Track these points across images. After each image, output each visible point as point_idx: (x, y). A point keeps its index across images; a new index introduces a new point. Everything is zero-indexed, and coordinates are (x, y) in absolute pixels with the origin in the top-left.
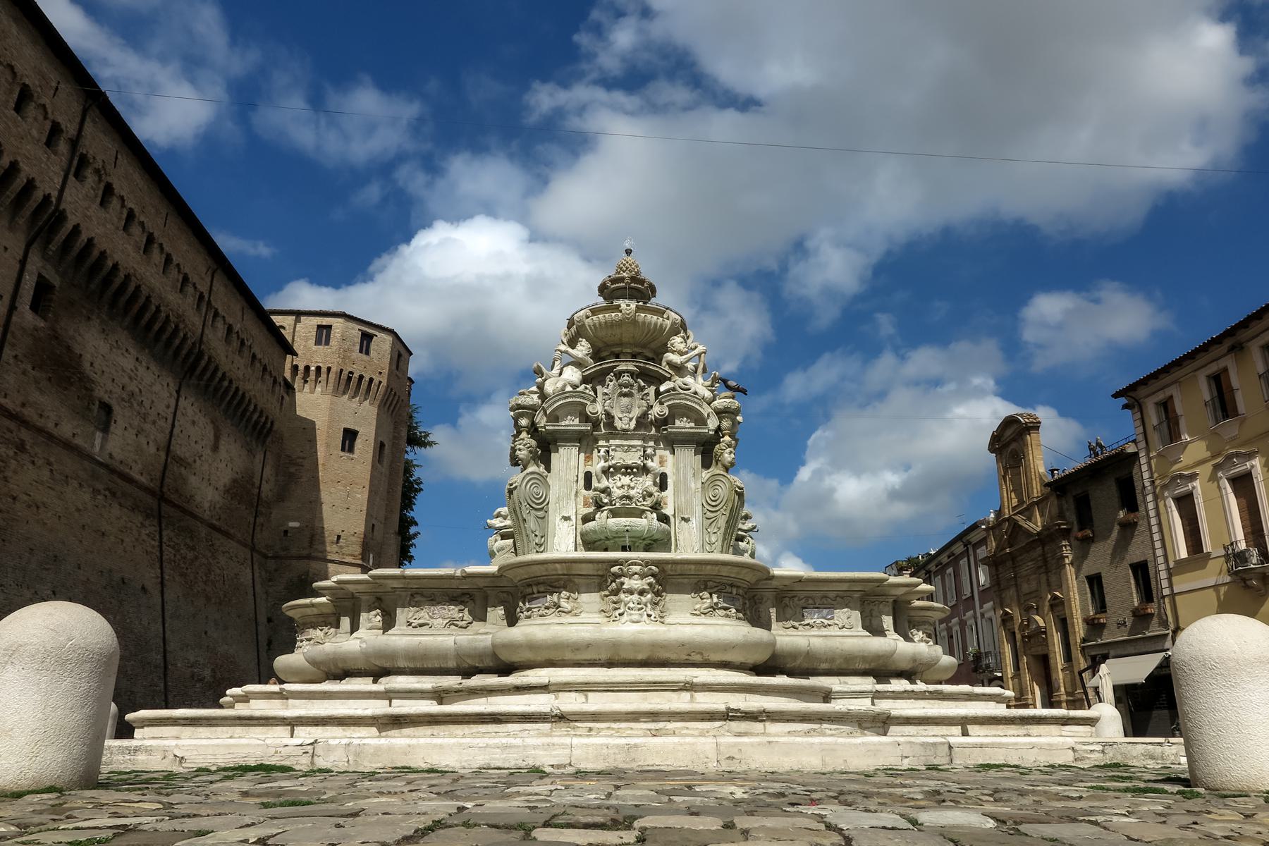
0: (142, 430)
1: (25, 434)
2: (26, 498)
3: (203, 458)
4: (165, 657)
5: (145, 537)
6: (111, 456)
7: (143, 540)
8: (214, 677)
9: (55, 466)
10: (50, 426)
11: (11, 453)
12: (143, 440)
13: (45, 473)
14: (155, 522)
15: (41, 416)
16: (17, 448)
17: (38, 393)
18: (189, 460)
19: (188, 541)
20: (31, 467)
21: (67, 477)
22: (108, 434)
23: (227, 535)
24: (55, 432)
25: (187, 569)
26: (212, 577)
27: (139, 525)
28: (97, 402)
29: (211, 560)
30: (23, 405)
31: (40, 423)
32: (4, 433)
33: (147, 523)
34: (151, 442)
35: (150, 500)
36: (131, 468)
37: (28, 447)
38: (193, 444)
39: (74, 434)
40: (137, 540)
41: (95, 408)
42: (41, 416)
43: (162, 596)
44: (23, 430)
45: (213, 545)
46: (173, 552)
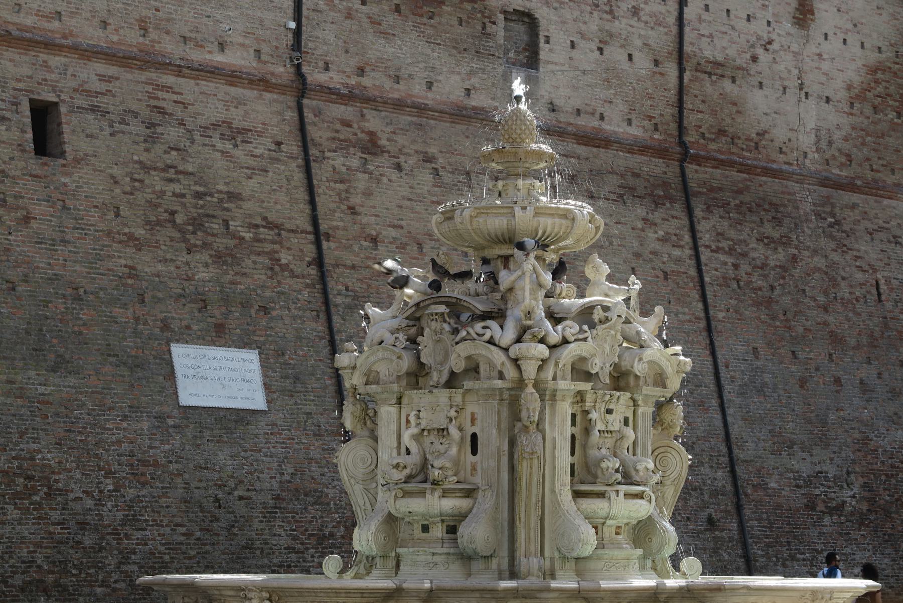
0: (611, 35)
1: (374, 121)
2: (393, 233)
3: (775, 46)
4: (733, 472)
5: (657, 246)
6: (553, 108)
7: (654, 253)
8: (871, 501)
9: (441, 160)
10: (418, 90)
11: (355, 163)
12: (613, 53)
13: (425, 177)
14: (678, 209)
15: (397, 79)
16: (365, 150)
17: (383, 41)
18: (739, 62)
19: (768, 229)
20: (394, 175)
21: (468, 173)
22: (537, 69)
23: (874, 189)
24: (430, 98)
25: (772, 288)
26: (844, 291)
27: (640, 225)
28: (501, 17)
29: (835, 257)
30: (361, 72)
31: (396, 92)
32: (337, 131)
33: (657, 216)
34: (637, 55)
35: (656, 167)
36: (602, 118)
37: (383, 142)
38: (741, 24)
39: (468, 91)
40: (637, 255)
41: (499, 29)
42: (397, 79)
43: (713, 354)
44: (369, 113)
45: (838, 223)
46: (730, 260)
